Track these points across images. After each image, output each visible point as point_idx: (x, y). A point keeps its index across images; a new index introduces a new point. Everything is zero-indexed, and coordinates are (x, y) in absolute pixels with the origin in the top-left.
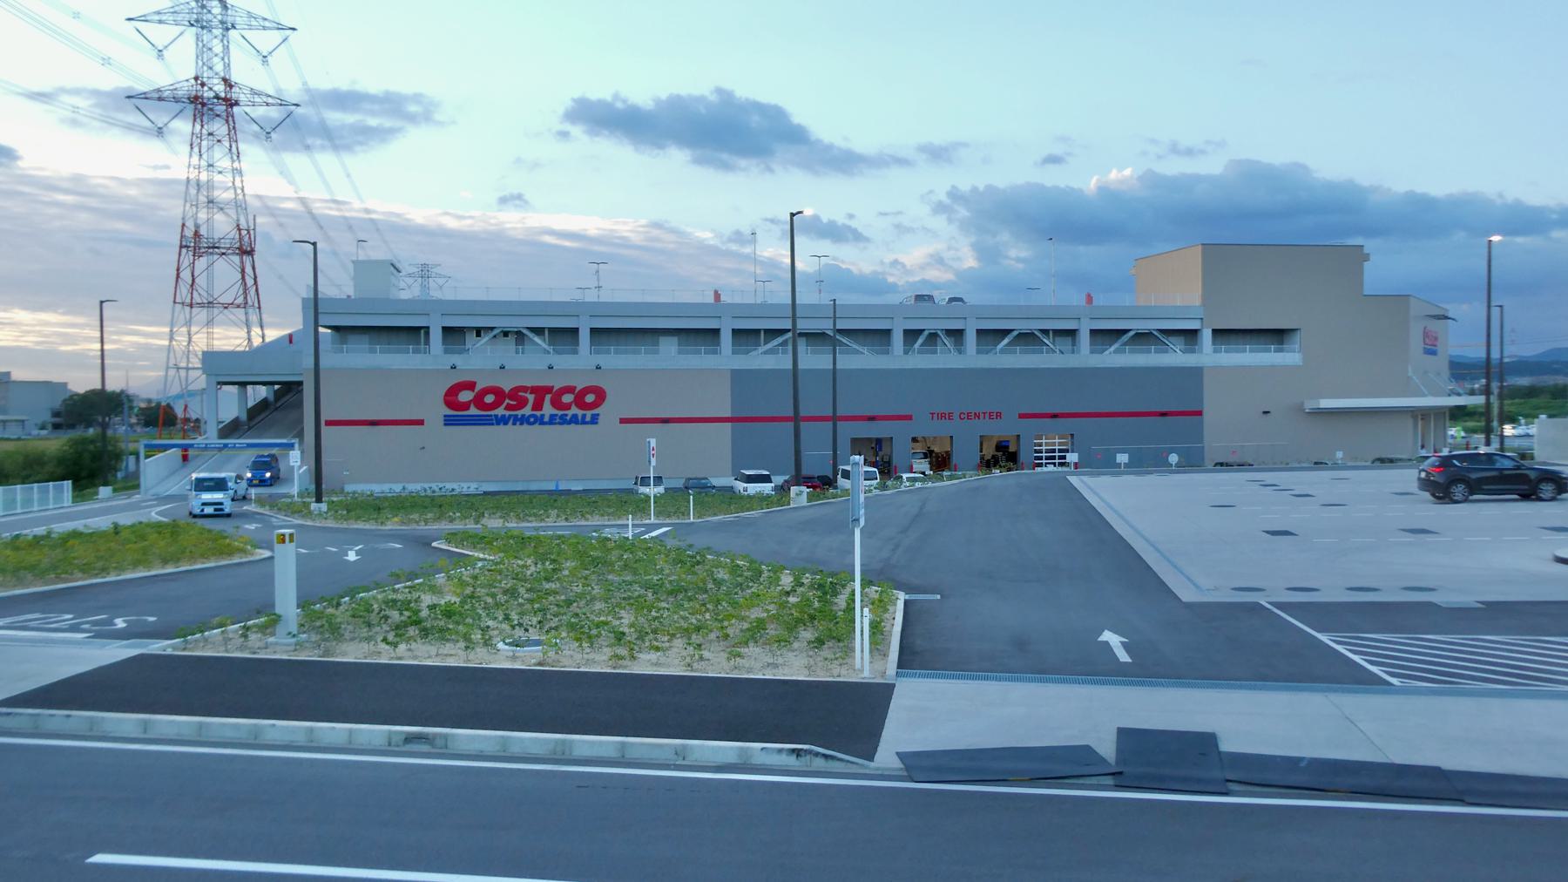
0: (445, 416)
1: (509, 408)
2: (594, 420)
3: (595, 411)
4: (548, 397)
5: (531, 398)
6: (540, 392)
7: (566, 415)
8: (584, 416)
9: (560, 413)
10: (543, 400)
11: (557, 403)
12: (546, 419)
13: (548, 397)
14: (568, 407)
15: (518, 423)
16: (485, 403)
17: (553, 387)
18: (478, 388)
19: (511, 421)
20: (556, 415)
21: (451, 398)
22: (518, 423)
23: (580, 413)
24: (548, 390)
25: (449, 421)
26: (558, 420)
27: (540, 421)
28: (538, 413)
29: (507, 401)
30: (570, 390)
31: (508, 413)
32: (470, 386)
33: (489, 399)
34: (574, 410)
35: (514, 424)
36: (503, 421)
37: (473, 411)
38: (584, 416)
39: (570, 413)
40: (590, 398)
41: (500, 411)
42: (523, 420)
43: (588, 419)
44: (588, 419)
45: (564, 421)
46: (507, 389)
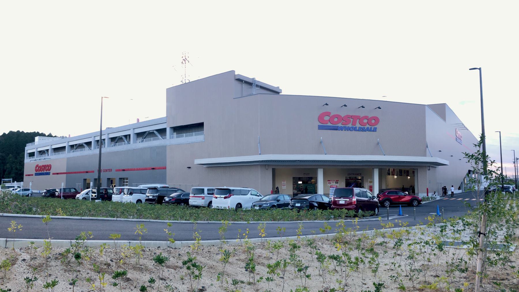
0: (319, 126)
2: (375, 130)
3: (375, 127)
4: (358, 120)
5: (352, 120)
6: (355, 118)
8: (371, 128)
9: (363, 127)
10: (356, 123)
12: (358, 129)
17: (360, 116)
19: (344, 130)
20: (361, 128)
21: (321, 118)
23: (370, 127)
24: (358, 117)
25: (320, 128)
27: (355, 129)
28: (354, 126)
30: (366, 117)
32: (328, 114)
33: (336, 120)
34: (368, 126)
35: (345, 130)
36: (341, 129)
37: (329, 124)
38: (371, 128)
42: (349, 129)
43: (373, 129)
44: (373, 129)
45: (363, 130)
46: (343, 116)
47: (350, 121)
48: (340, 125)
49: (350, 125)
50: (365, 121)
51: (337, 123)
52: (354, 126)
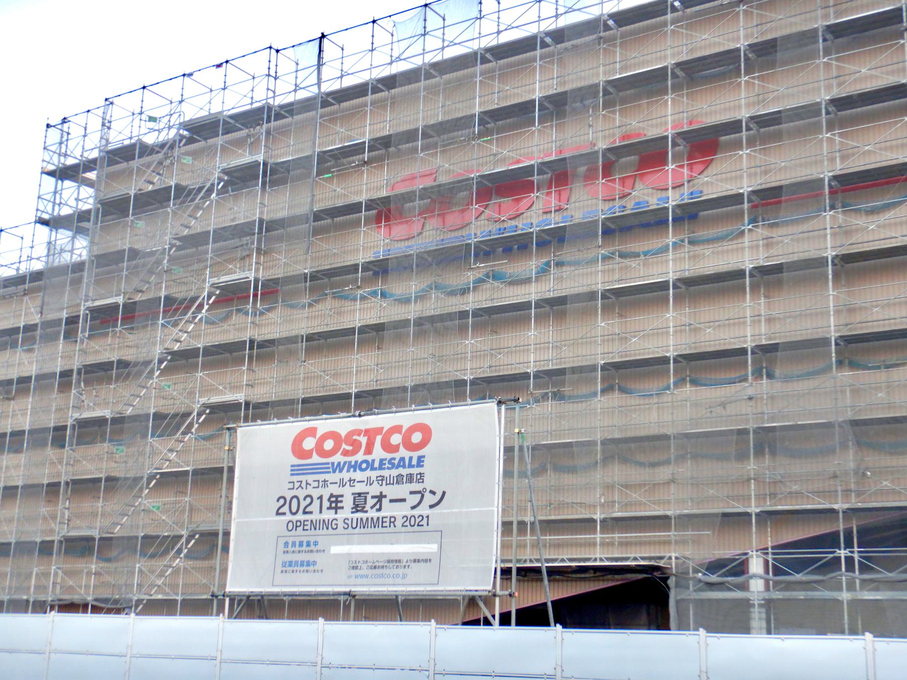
0: (292, 466)
1: (346, 453)
4: (379, 438)
5: (364, 440)
7: (394, 459)
8: (411, 458)
9: (389, 456)
11: (388, 447)
12: (376, 465)
13: (379, 438)
14: (395, 449)
15: (352, 469)
16: (329, 451)
17: (382, 428)
18: (319, 434)
22: (352, 469)
26: (387, 465)
29: (344, 446)
37: (316, 459)
39: (397, 456)
40: (417, 438)
41: (338, 458)
47: (360, 444)
48: (338, 458)
49: (360, 457)
50: (396, 439)
51: (332, 452)
52: (369, 458)
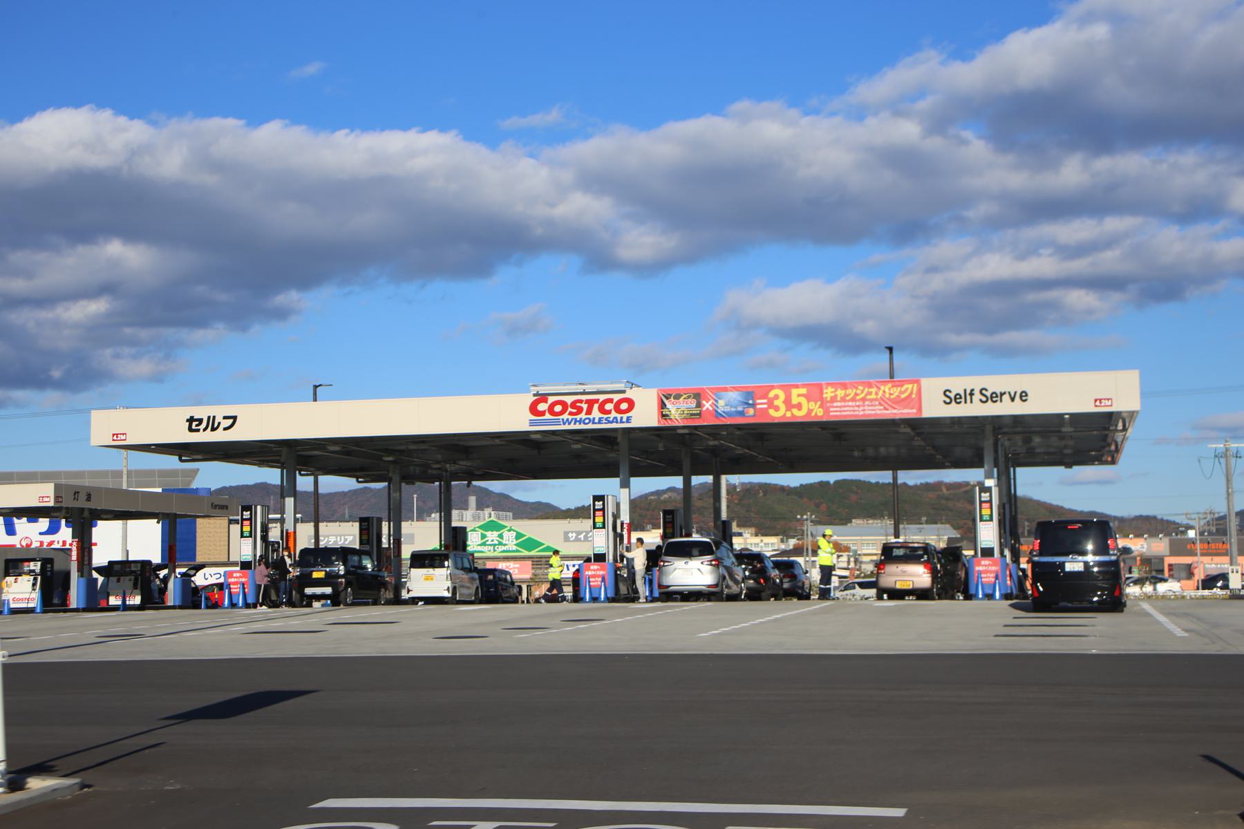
1: (571, 414)
3: (628, 415)
4: (596, 406)
5: (585, 406)
8: (622, 418)
9: (606, 416)
10: (593, 406)
11: (602, 410)
13: (596, 406)
14: (609, 412)
19: (573, 422)
22: (578, 423)
23: (619, 416)
31: (570, 417)
33: (558, 408)
34: (614, 414)
40: (624, 406)
43: (624, 420)
